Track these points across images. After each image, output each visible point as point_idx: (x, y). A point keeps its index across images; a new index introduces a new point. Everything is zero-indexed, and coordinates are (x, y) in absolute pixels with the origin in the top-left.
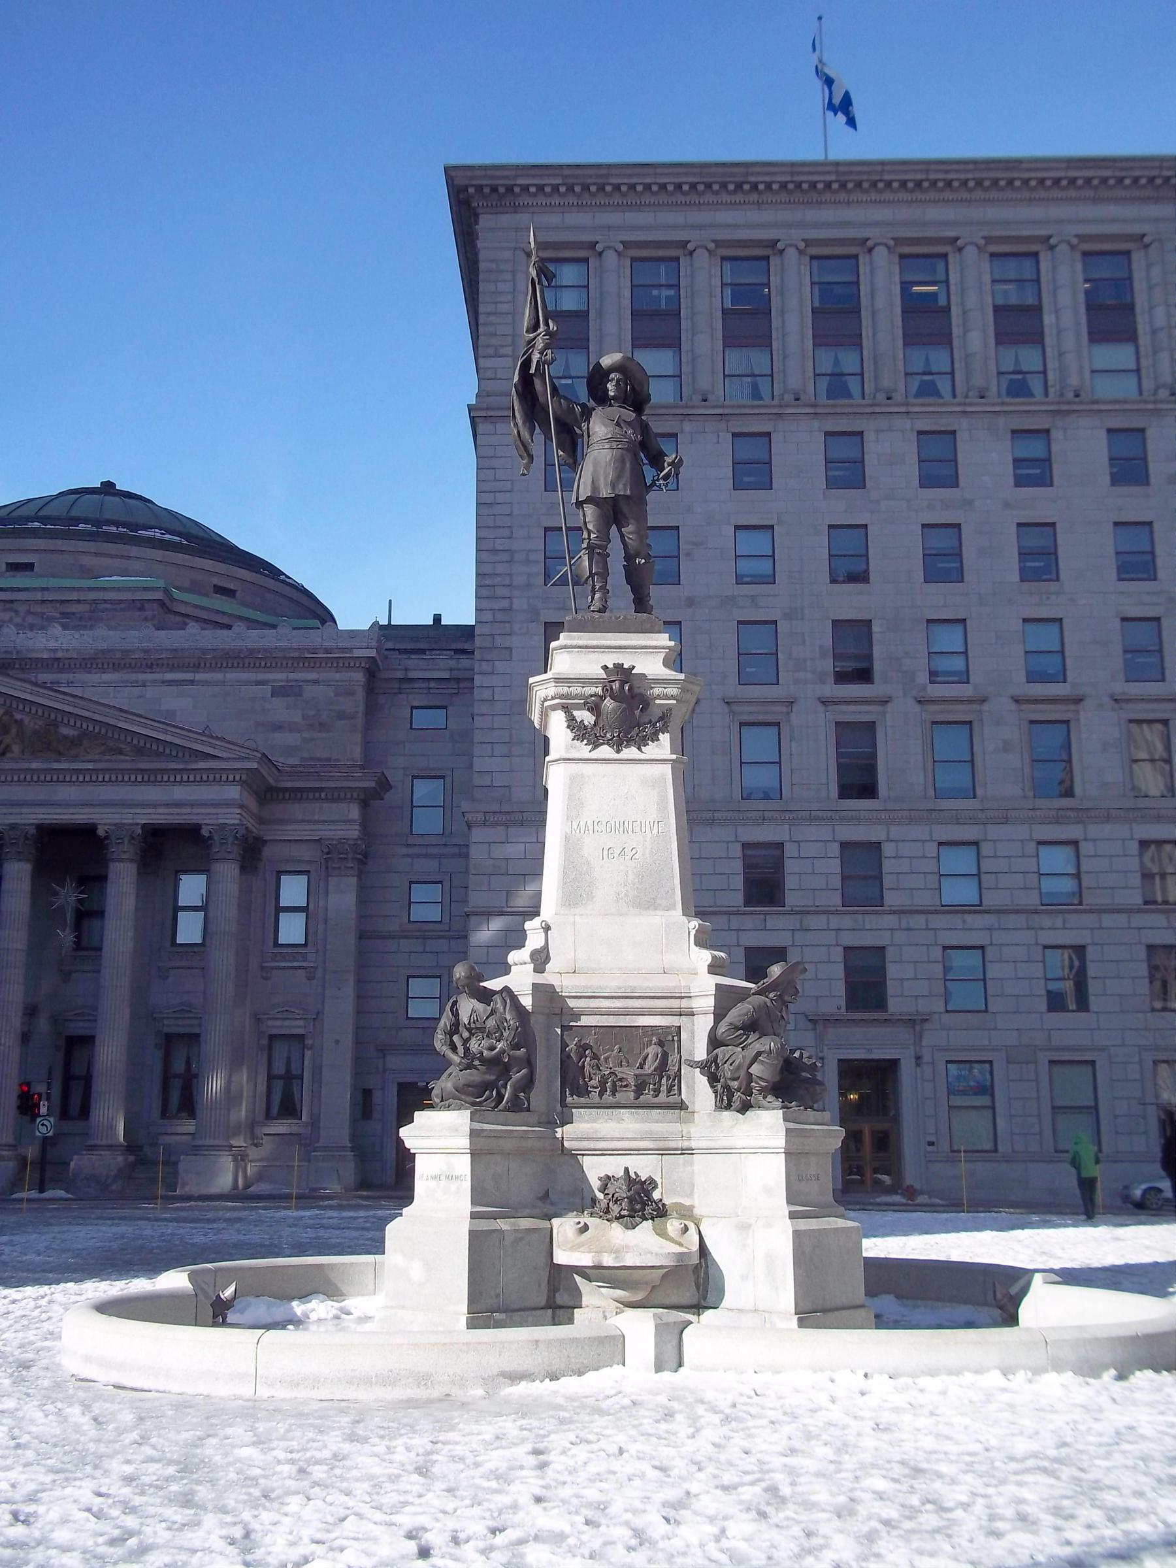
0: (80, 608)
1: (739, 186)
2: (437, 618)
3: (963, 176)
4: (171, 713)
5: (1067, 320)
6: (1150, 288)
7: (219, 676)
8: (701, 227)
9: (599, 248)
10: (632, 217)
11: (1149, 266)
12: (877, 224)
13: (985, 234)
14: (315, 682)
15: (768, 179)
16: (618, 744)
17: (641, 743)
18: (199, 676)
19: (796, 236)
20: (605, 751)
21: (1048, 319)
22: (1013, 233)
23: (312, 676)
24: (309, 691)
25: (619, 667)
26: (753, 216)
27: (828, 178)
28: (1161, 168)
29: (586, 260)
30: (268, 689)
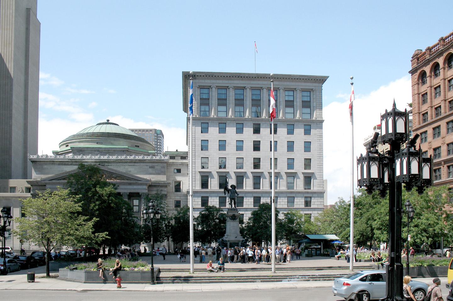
0: (112, 151)
1: (239, 77)
2: (177, 150)
3: (280, 77)
4: (130, 171)
5: (298, 104)
6: (313, 99)
7: (139, 164)
8: (231, 84)
9: (211, 87)
10: (218, 81)
11: (313, 94)
12: (264, 84)
13: (284, 87)
14: (158, 166)
15: (244, 76)
16: (233, 220)
17: (235, 220)
18: (135, 164)
19: (249, 86)
20: (232, 221)
21: (295, 103)
22: (289, 87)
23: (156, 164)
24: (156, 167)
25: (234, 215)
26: (241, 82)
27: (255, 76)
28: (316, 78)
29: (209, 88)
30: (148, 167)
